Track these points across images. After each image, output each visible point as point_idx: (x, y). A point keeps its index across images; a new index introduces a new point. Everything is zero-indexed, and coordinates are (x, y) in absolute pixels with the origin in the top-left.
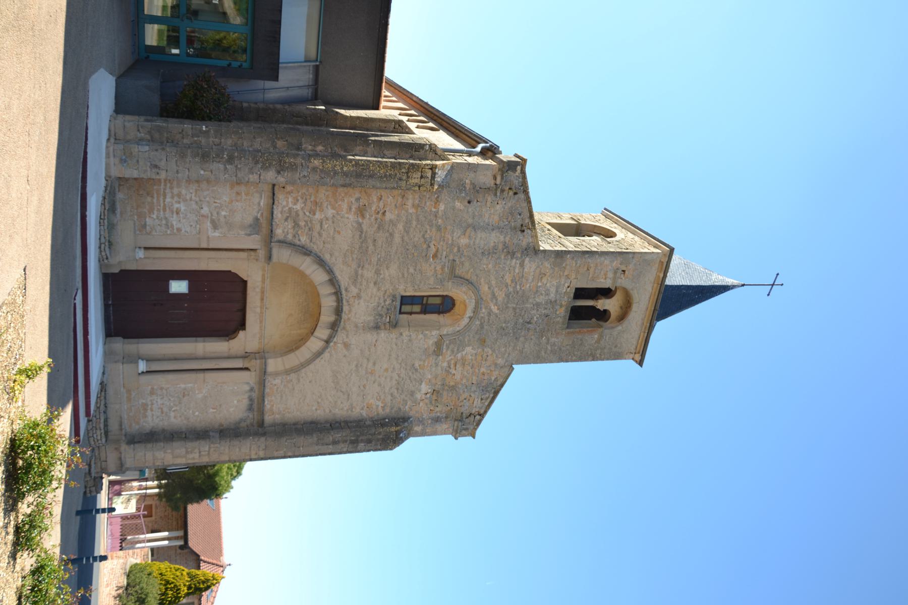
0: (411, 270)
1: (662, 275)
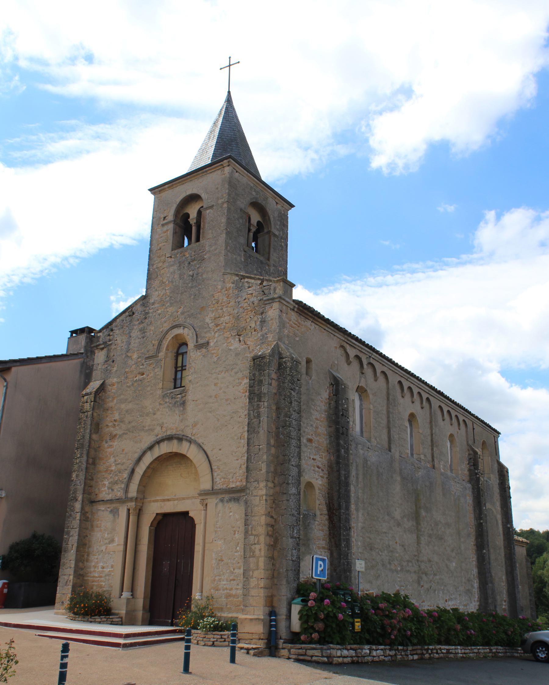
0: (149, 389)
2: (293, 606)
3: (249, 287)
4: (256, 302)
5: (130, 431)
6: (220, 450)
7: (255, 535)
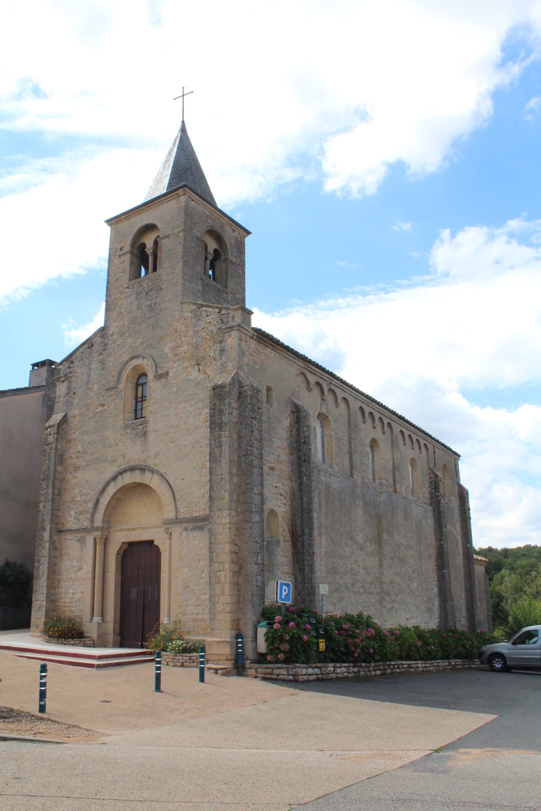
0: (110, 420)
1: (123, 217)
2: (259, 629)
3: (207, 316)
4: (215, 331)
5: (93, 462)
6: (183, 479)
7: (220, 563)
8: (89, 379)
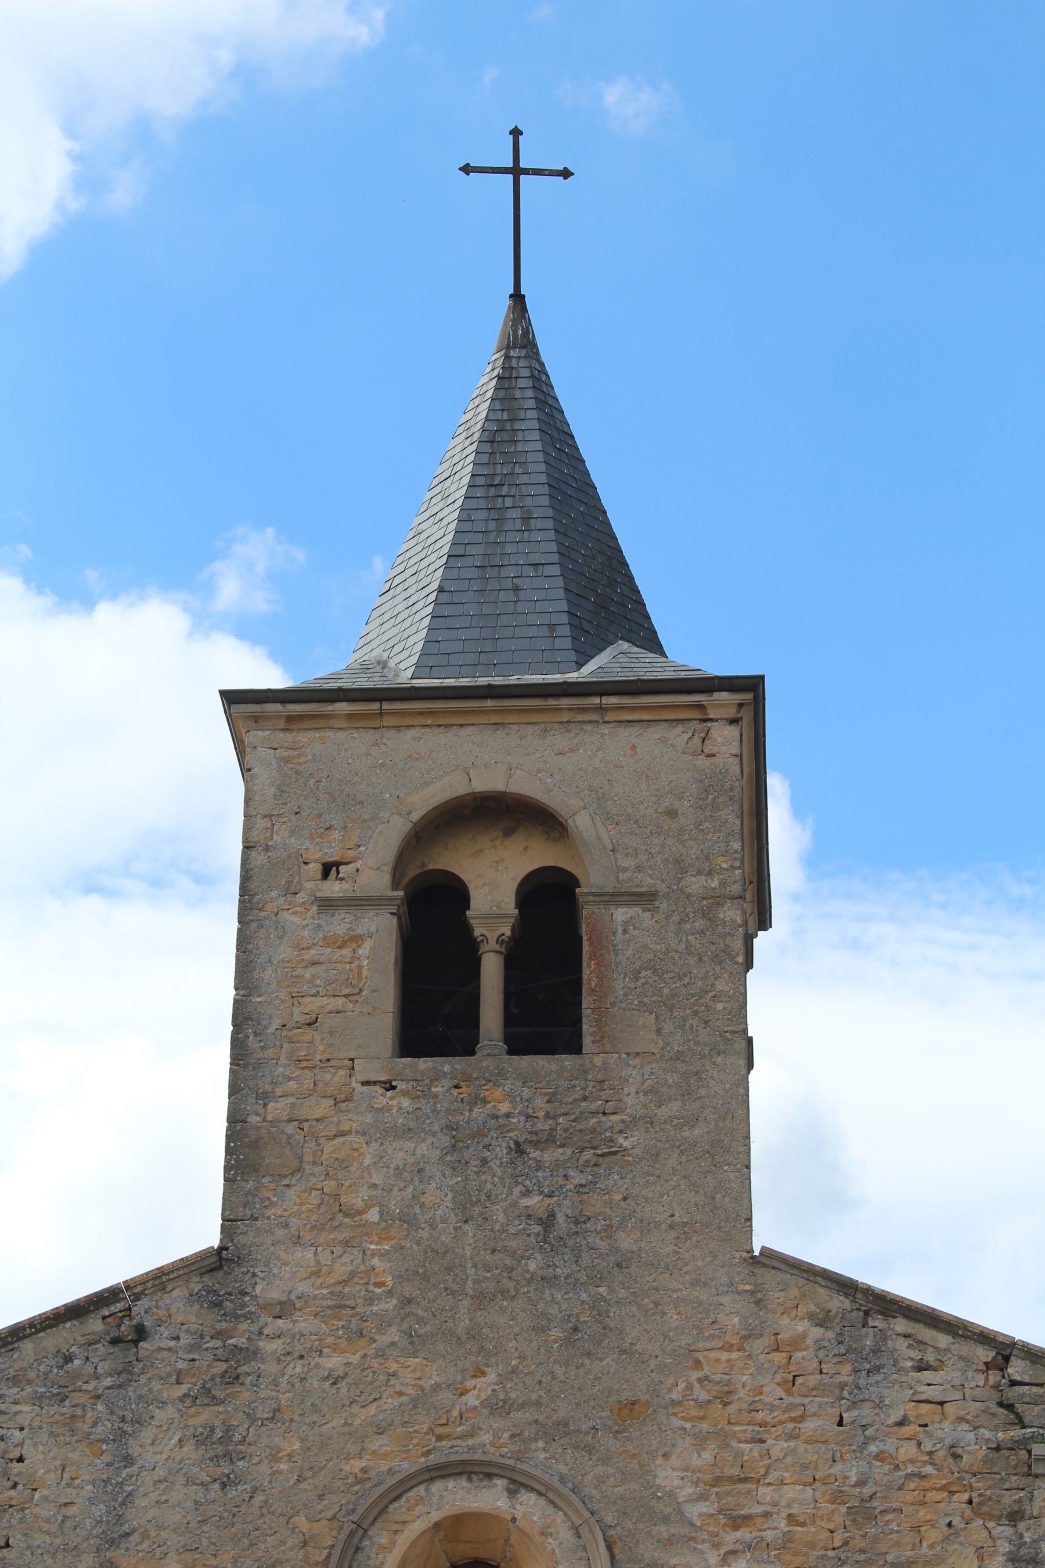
1: (343, 707)
3: (922, 1367)
4: (974, 1452)
8: (119, 1519)
